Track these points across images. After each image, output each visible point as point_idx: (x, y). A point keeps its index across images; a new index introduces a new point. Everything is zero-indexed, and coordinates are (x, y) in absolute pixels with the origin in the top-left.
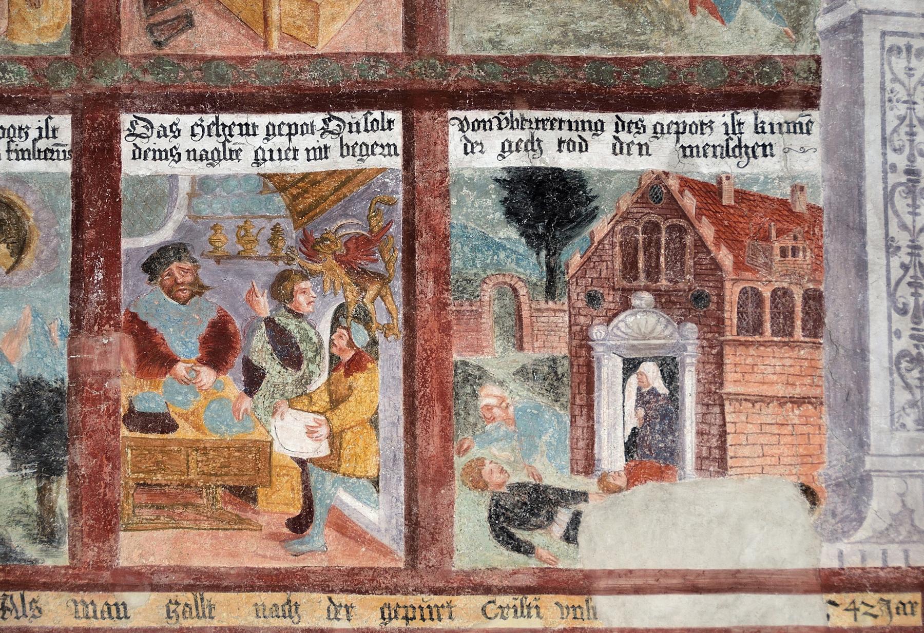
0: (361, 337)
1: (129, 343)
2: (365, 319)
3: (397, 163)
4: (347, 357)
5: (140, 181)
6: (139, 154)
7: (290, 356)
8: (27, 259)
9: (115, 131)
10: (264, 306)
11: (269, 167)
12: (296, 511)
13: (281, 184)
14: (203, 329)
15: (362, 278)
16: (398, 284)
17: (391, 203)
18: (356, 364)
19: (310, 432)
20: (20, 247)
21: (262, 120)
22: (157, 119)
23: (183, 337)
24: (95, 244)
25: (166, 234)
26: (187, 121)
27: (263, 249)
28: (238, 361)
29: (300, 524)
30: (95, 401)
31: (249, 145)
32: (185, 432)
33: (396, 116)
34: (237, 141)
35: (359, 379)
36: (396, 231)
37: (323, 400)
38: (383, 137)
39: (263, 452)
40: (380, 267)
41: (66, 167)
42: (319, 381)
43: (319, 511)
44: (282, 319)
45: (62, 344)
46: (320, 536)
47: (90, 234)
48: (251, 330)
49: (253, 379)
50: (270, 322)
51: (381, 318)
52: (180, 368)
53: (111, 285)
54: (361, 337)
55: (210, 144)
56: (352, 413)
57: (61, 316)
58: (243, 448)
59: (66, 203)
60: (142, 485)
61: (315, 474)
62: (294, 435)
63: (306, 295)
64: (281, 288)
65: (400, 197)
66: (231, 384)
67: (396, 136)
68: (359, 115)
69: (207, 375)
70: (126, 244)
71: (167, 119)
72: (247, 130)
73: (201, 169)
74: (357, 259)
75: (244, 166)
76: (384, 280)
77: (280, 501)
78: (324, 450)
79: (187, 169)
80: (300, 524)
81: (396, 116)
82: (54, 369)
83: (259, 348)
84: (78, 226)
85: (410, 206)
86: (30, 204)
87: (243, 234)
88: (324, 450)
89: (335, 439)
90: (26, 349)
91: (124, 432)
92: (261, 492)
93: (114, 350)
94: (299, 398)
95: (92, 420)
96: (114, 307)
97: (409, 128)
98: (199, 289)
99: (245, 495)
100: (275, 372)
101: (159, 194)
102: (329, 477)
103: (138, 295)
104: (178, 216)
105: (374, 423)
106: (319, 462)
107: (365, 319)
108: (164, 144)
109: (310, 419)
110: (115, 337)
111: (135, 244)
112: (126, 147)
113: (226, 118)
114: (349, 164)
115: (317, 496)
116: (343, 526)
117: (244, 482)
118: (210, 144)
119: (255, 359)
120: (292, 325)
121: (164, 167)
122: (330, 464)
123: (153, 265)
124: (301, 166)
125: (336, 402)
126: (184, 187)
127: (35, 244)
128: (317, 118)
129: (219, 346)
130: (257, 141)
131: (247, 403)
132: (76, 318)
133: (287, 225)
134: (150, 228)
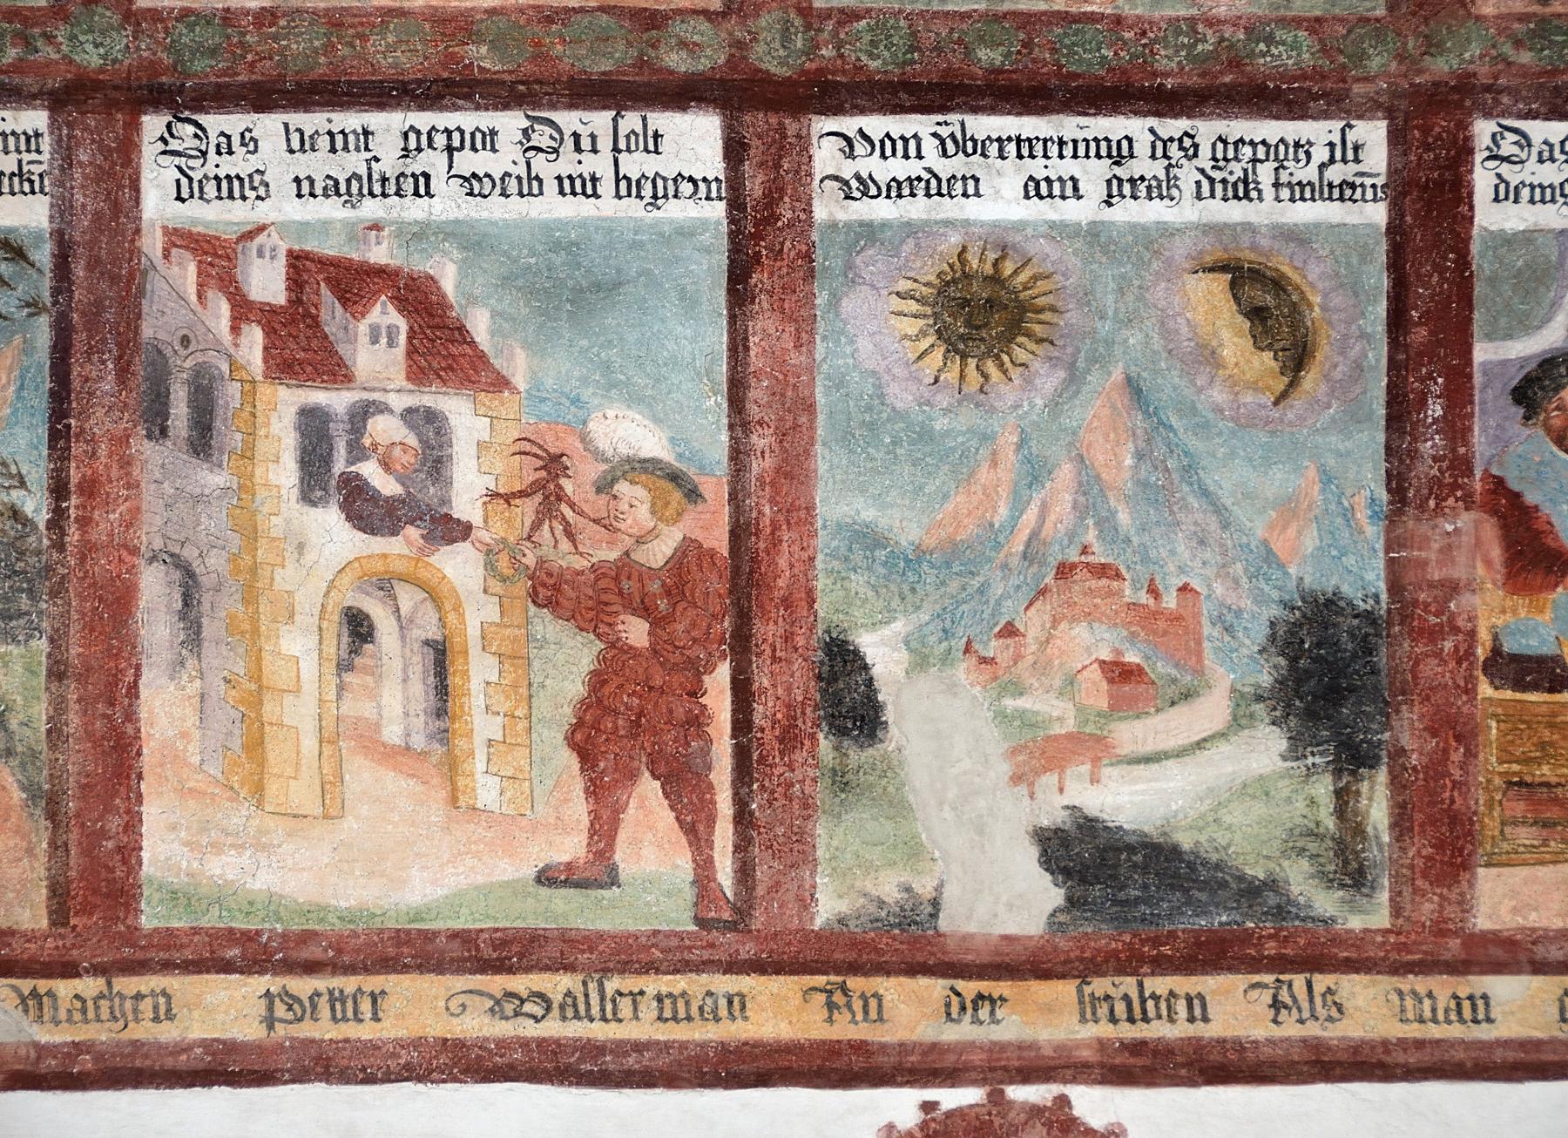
1: (1490, 530)
5: (1508, 241)
6: (1505, 193)
8: (1310, 379)
20: (1297, 358)
24: (1427, 352)
30: (1434, 634)
41: (1377, 214)
45: (1374, 533)
47: (1419, 335)
53: (1456, 427)
57: (1368, 480)
59: (1378, 279)
60: (1517, 785)
70: (1482, 353)
82: (1363, 577)
84: (1397, 321)
86: (1314, 280)
90: (1310, 542)
91: (1485, 689)
93: (1465, 543)
95: (1429, 668)
96: (1463, 466)
103: (1502, 442)
110: (1466, 520)
111: (1497, 353)
112: (1483, 179)
123: (1532, 389)
127: (1324, 352)
132: (1397, 484)
134: (1525, 325)
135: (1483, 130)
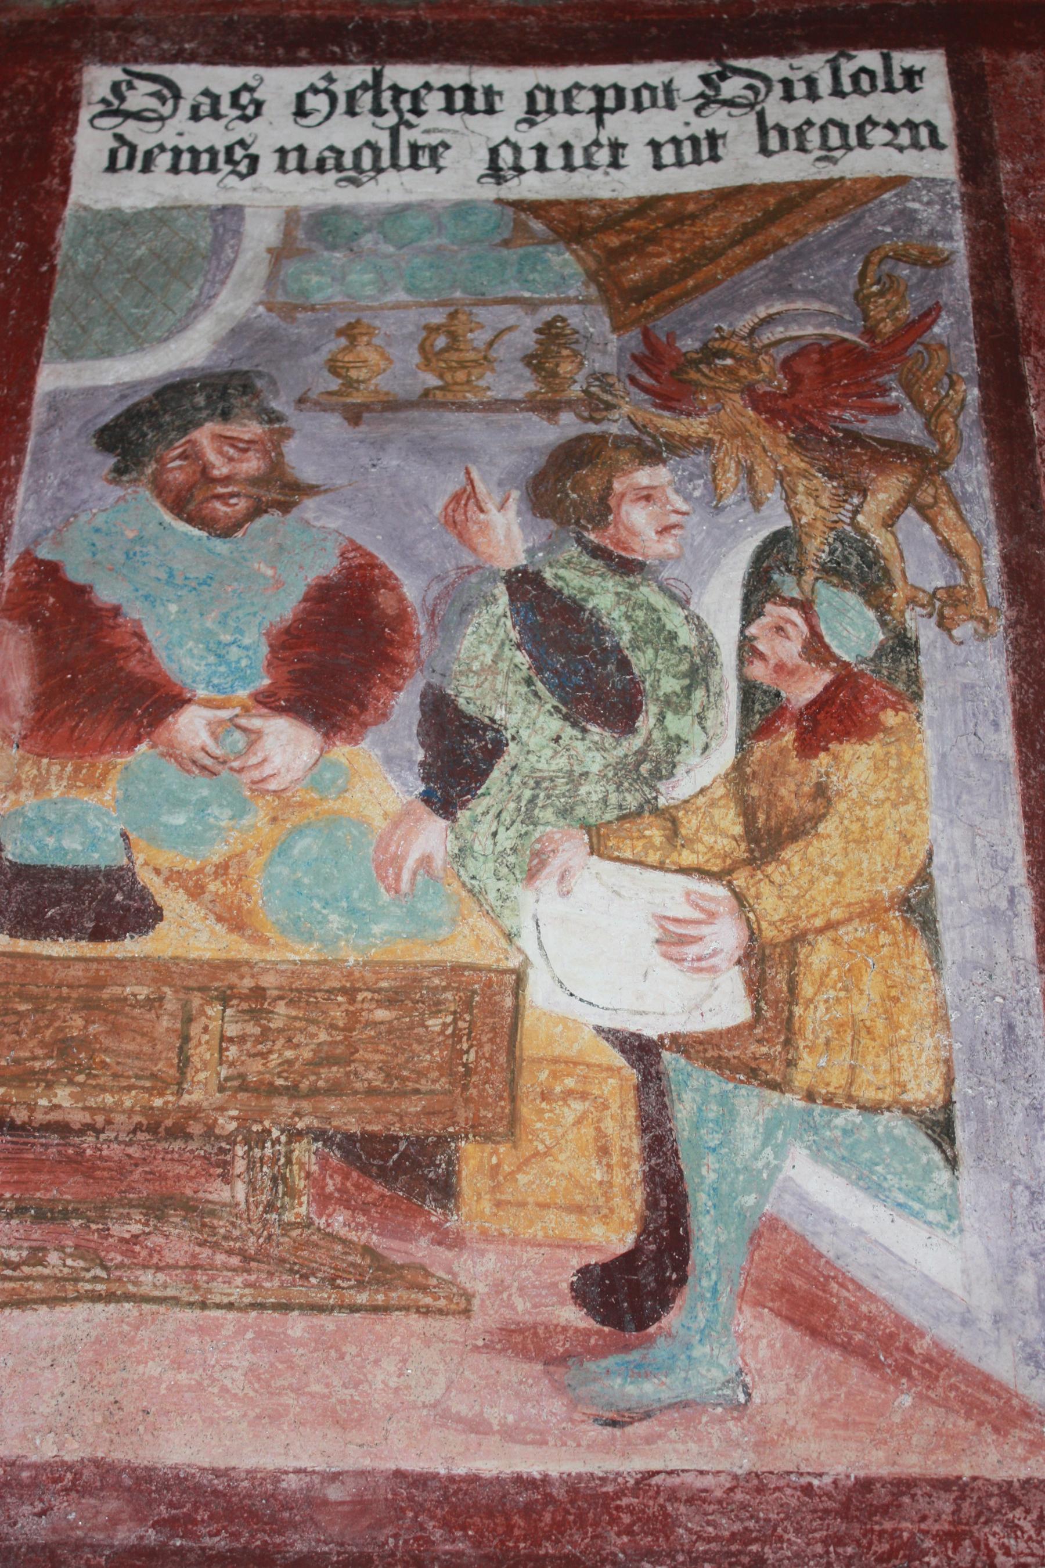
0: (853, 630)
2: (865, 574)
3: (943, 165)
4: (807, 688)
5: (122, 222)
7: (592, 680)
9: (65, 106)
10: (508, 535)
11: (532, 186)
12: (615, 1236)
13: (570, 223)
14: (286, 606)
15: (852, 461)
16: (973, 474)
17: (932, 261)
18: (843, 712)
19: (674, 940)
21: (514, 82)
22: (192, 78)
23: (207, 612)
25: (190, 350)
26: (281, 83)
27: (512, 381)
28: (405, 704)
29: (633, 1291)
31: (470, 140)
32: (187, 934)
33: (932, 63)
34: (434, 123)
35: (853, 765)
36: (955, 331)
37: (722, 830)
38: (896, 107)
39: (488, 1007)
40: (910, 427)
42: (706, 764)
43: (711, 1238)
44: (571, 576)
46: (718, 1339)
48: (456, 604)
49: (458, 759)
50: (524, 585)
51: (918, 560)
52: (191, 726)
54: (853, 630)
55: (349, 133)
56: (825, 875)
58: (407, 991)
61: (693, 1095)
62: (608, 948)
63: (652, 503)
64: (568, 487)
65: (958, 245)
66: (378, 772)
67: (934, 100)
68: (815, 63)
69: (288, 746)
70: (52, 377)
71: (225, 78)
72: (464, 102)
73: (319, 191)
74: (823, 403)
75: (459, 179)
76: (926, 464)
77: (550, 1198)
78: (724, 1003)
79: (271, 197)
80: (633, 1291)
81: (932, 63)
83: (485, 663)
85: (990, 269)
87: (446, 346)
88: (724, 1003)
89: (769, 965)
92: (473, 1159)
94: (633, 825)
97: (967, 90)
98: (281, 491)
99: (405, 1171)
100: (536, 732)
101: (178, 256)
102: (752, 1105)
104: (236, 301)
105: (917, 908)
106: (705, 1049)
107: (865, 574)
108: (210, 134)
109: (673, 894)
112: (90, 144)
113: (405, 75)
114: (790, 168)
115: (702, 1177)
116: (810, 1298)
117: (405, 1119)
118: (349, 133)
119: (471, 696)
120: (604, 596)
121: (203, 189)
122: (757, 1054)
123: (132, 435)
124: (637, 180)
125: (768, 837)
126: (261, 232)
128: (687, 76)
129: (338, 655)
130: (499, 127)
131: (433, 835)
133: (591, 321)
134: (137, 337)
135: (98, 79)
